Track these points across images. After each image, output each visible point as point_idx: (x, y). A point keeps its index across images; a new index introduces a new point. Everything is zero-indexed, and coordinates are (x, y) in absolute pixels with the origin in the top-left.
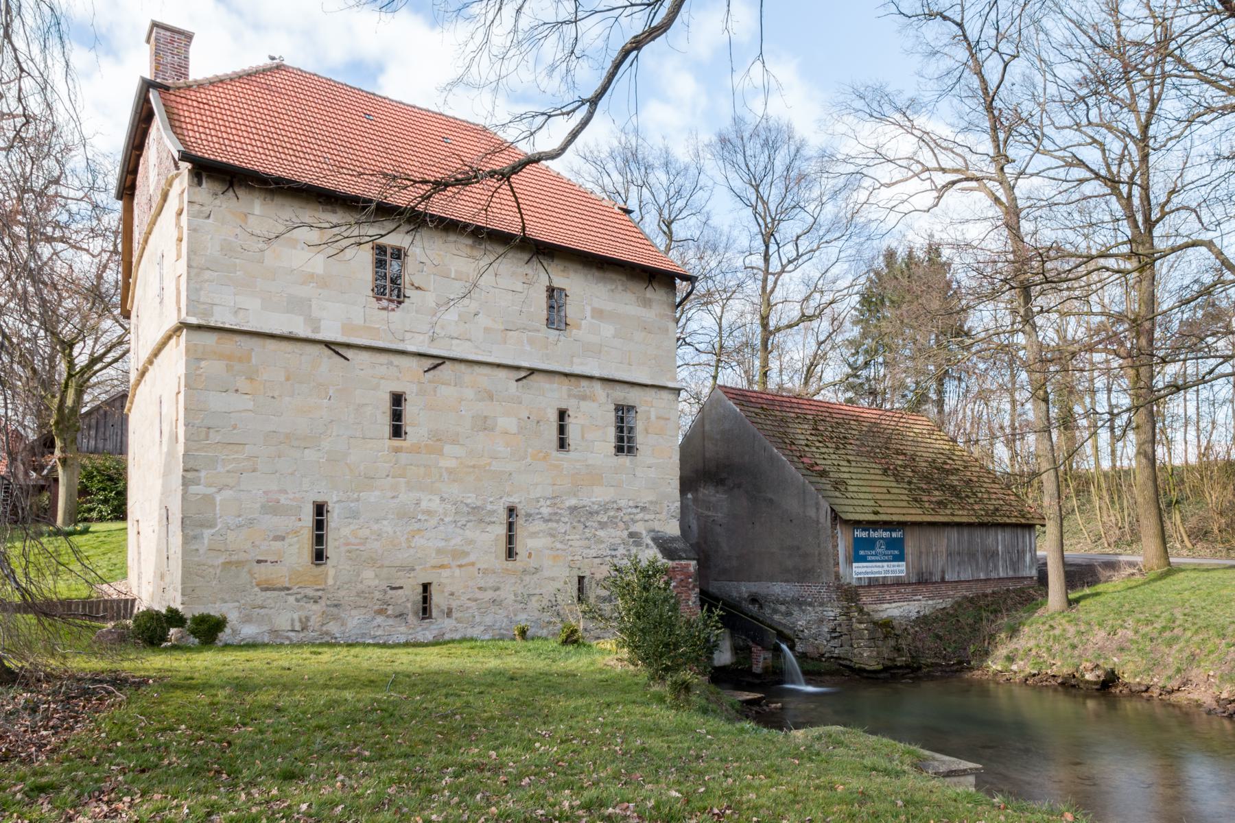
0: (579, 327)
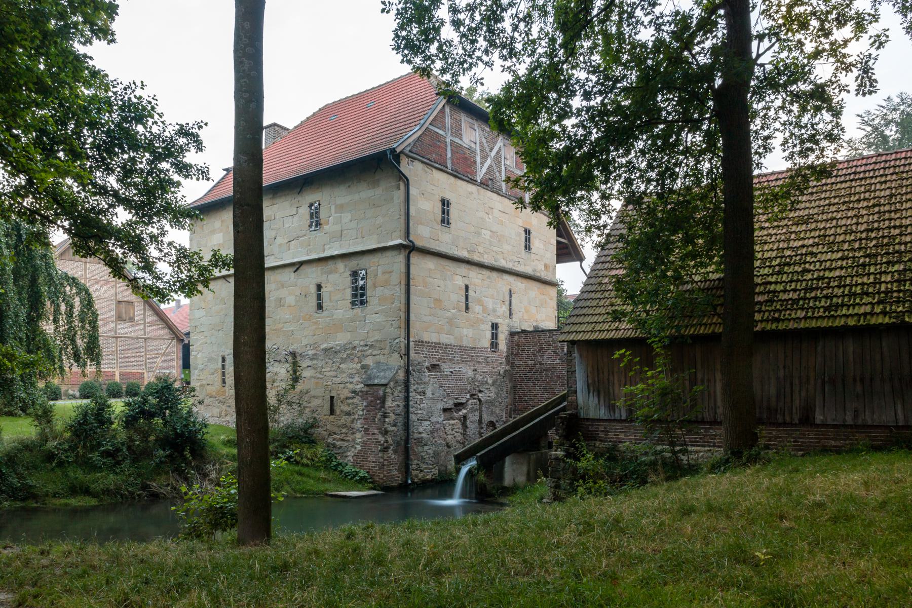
0: (328, 223)
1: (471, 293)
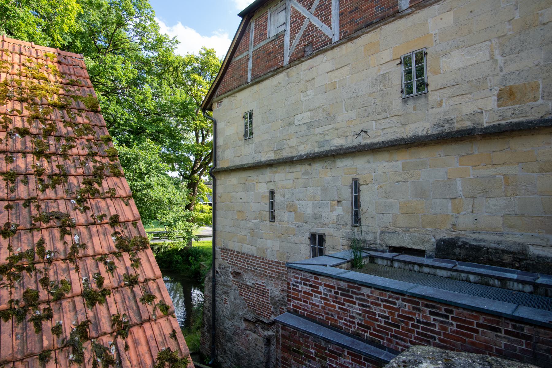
1: (277, 198)
